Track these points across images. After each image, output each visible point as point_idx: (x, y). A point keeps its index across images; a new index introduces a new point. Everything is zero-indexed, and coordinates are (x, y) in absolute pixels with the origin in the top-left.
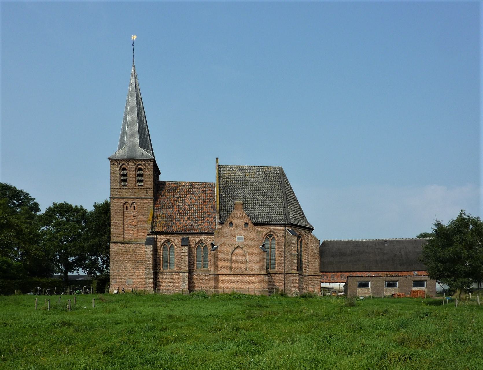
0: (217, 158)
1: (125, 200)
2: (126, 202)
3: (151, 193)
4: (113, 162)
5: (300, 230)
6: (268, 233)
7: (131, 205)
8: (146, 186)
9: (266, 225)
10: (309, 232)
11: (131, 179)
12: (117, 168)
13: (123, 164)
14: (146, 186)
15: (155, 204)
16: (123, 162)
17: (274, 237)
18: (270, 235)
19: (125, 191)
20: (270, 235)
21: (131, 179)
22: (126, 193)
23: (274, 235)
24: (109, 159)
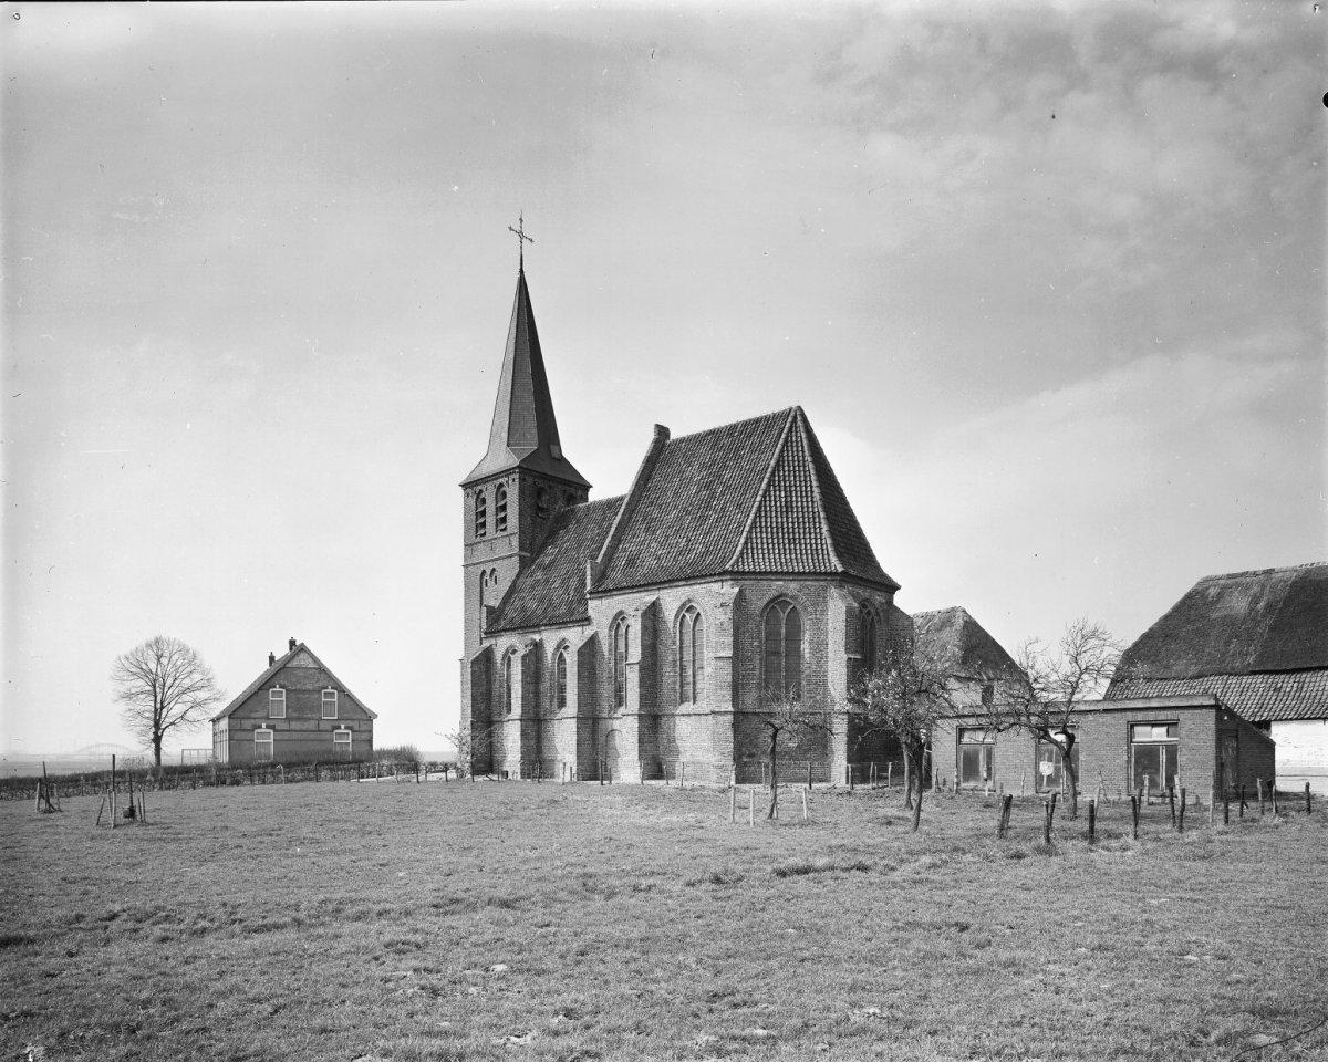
0: (658, 426)
1: (482, 567)
2: (484, 571)
3: (515, 541)
4: (469, 490)
5: (781, 583)
6: (684, 605)
7: (491, 576)
8: (509, 531)
9: (677, 584)
10: (822, 583)
11: (490, 519)
12: (472, 501)
13: (481, 491)
14: (509, 531)
15: (525, 564)
16: (480, 487)
17: (699, 614)
18: (690, 609)
19: (481, 546)
20: (690, 609)
21: (490, 519)
22: (482, 553)
23: (699, 610)
24: (462, 486)
